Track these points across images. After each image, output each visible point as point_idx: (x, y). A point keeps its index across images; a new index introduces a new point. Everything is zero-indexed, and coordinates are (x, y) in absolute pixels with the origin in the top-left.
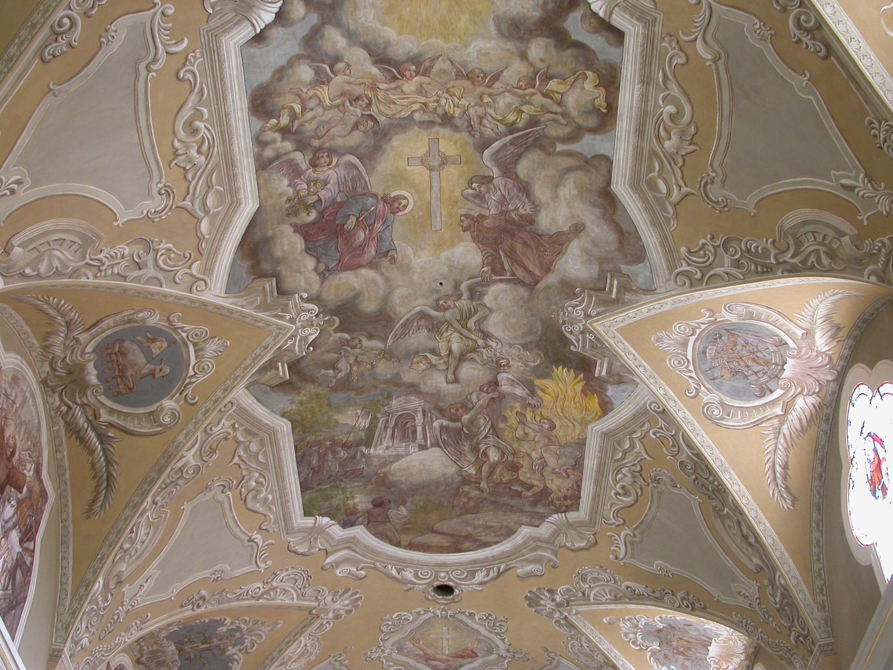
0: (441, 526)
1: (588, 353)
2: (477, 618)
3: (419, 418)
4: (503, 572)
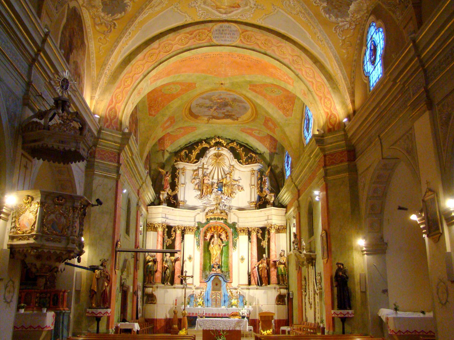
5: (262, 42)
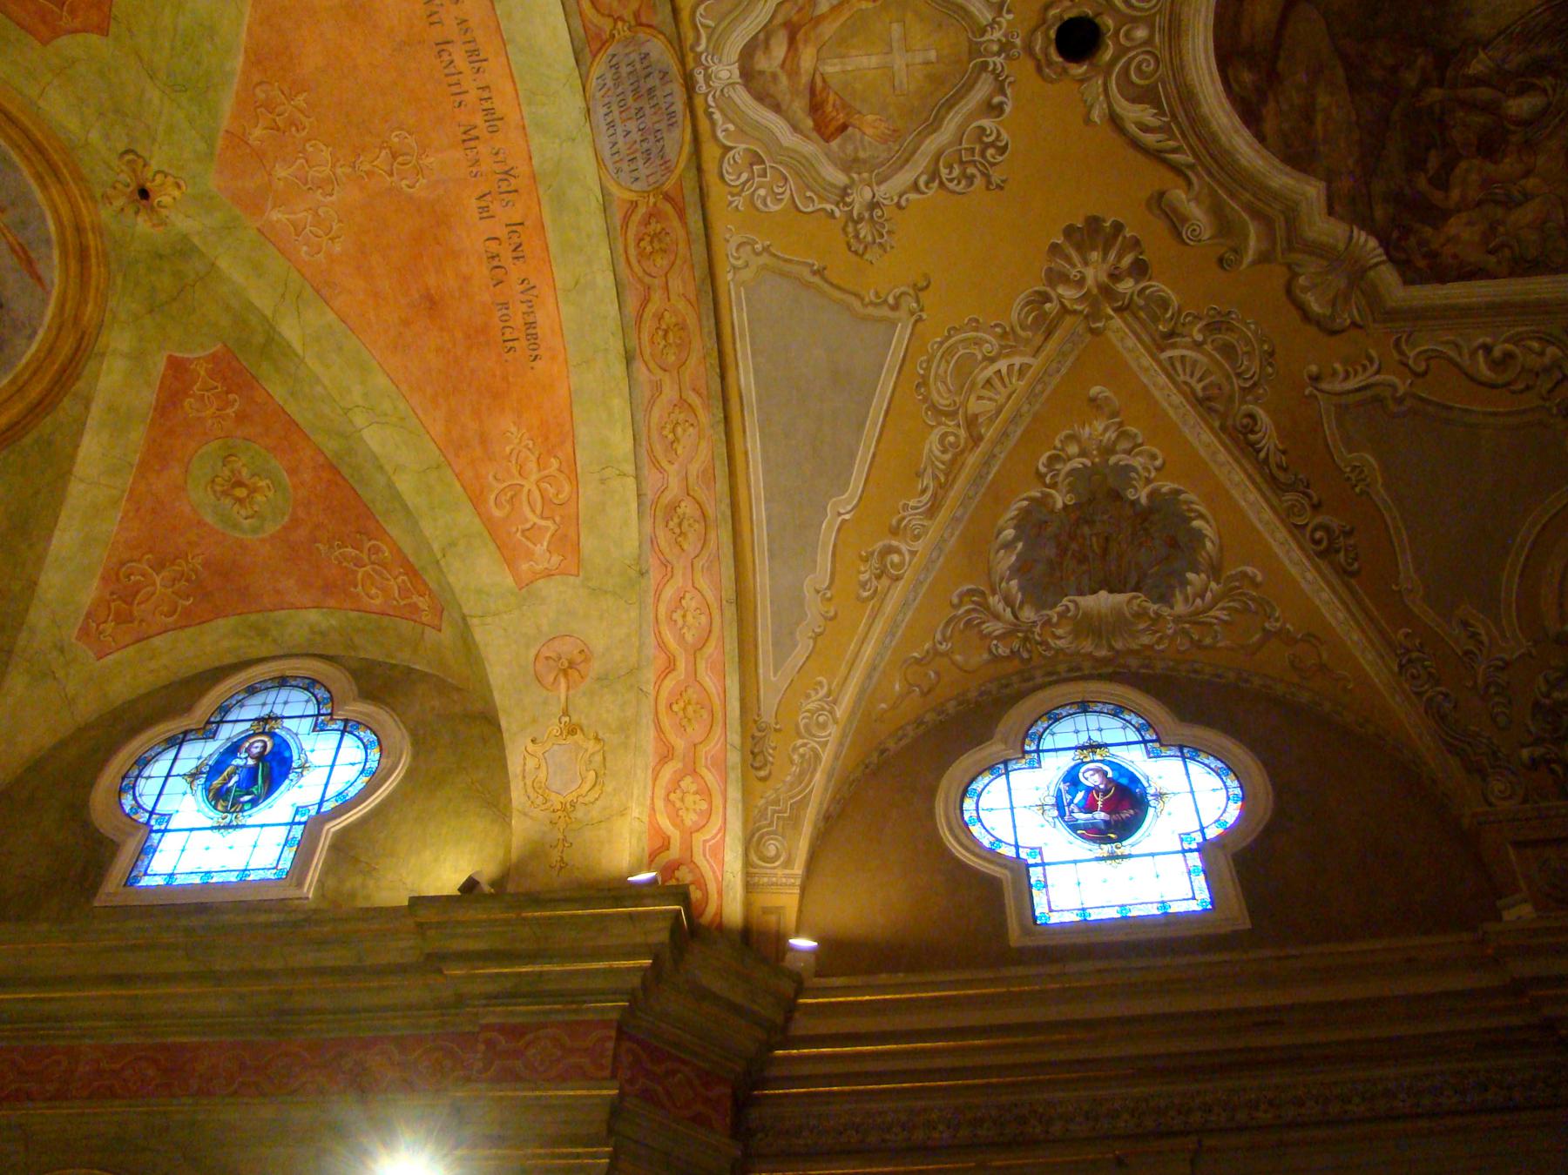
4: (1165, 162)
5: (667, 315)
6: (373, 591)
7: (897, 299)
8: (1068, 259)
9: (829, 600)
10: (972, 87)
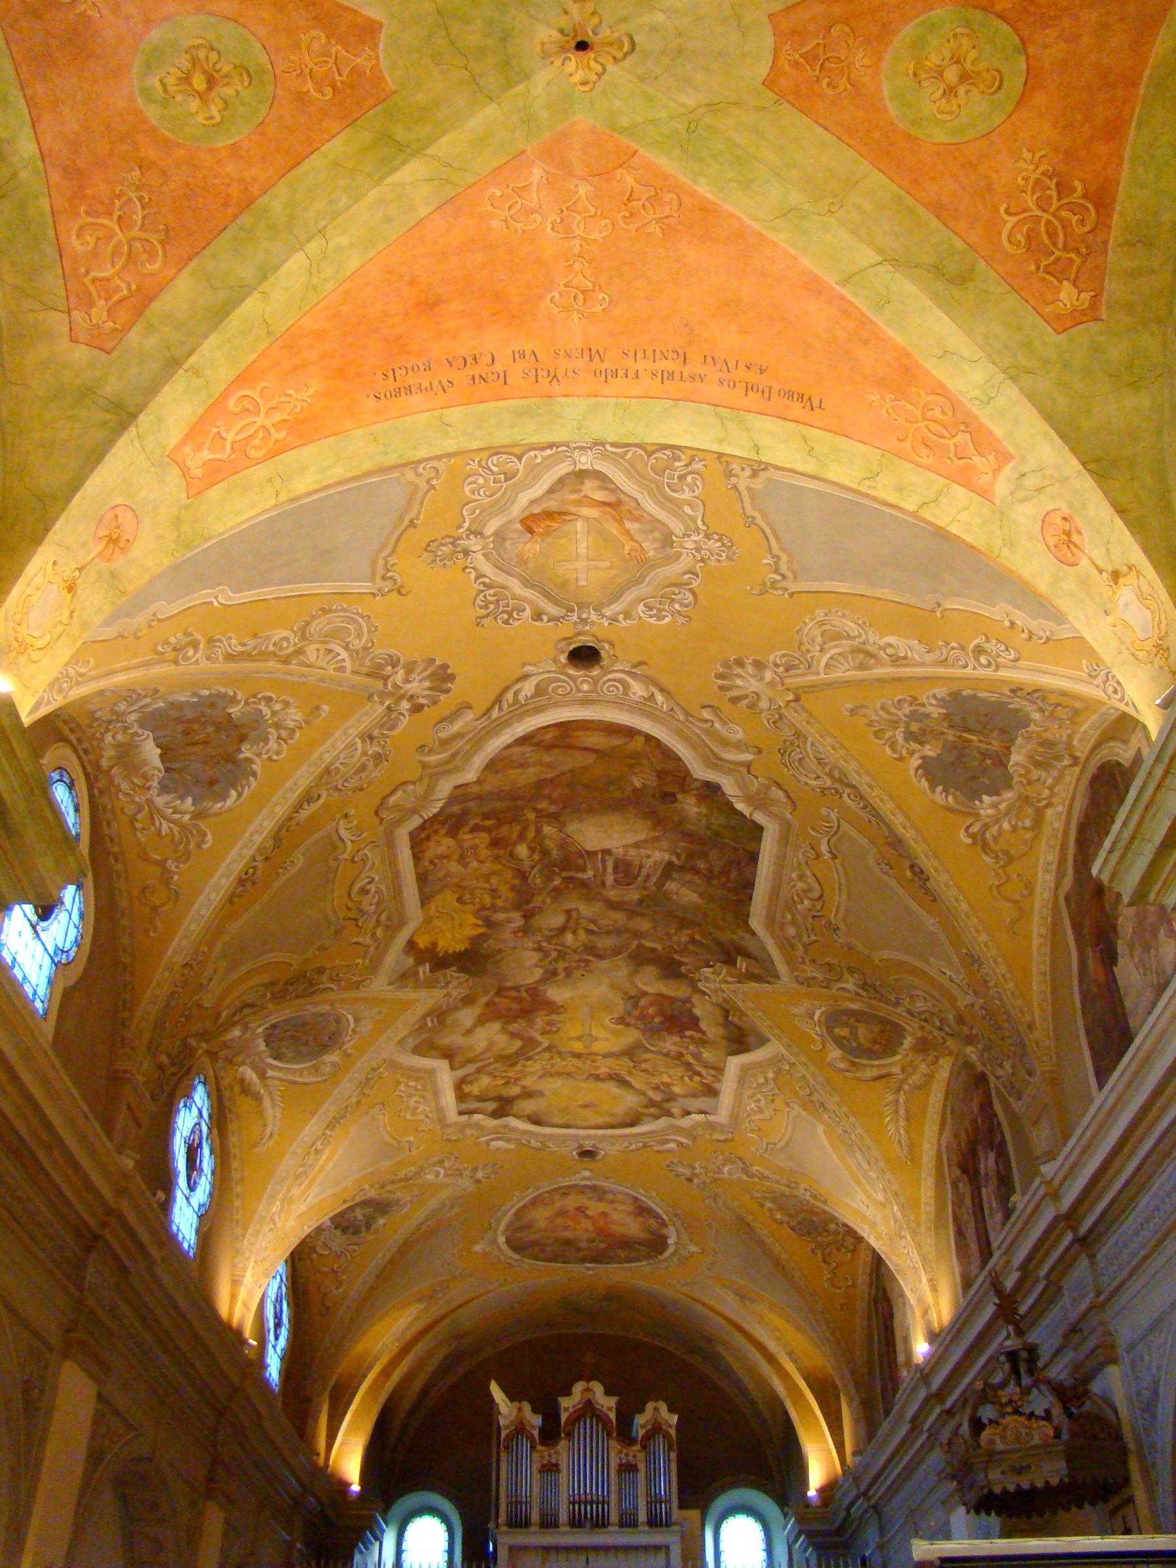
0: (590, 758)
1: (440, 974)
2: (528, 612)
3: (610, 879)
6: (90, 239)
7: (391, 578)
8: (425, 669)
9: (150, 627)
10: (555, 604)
